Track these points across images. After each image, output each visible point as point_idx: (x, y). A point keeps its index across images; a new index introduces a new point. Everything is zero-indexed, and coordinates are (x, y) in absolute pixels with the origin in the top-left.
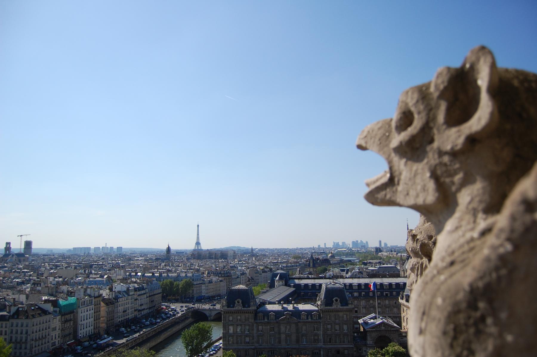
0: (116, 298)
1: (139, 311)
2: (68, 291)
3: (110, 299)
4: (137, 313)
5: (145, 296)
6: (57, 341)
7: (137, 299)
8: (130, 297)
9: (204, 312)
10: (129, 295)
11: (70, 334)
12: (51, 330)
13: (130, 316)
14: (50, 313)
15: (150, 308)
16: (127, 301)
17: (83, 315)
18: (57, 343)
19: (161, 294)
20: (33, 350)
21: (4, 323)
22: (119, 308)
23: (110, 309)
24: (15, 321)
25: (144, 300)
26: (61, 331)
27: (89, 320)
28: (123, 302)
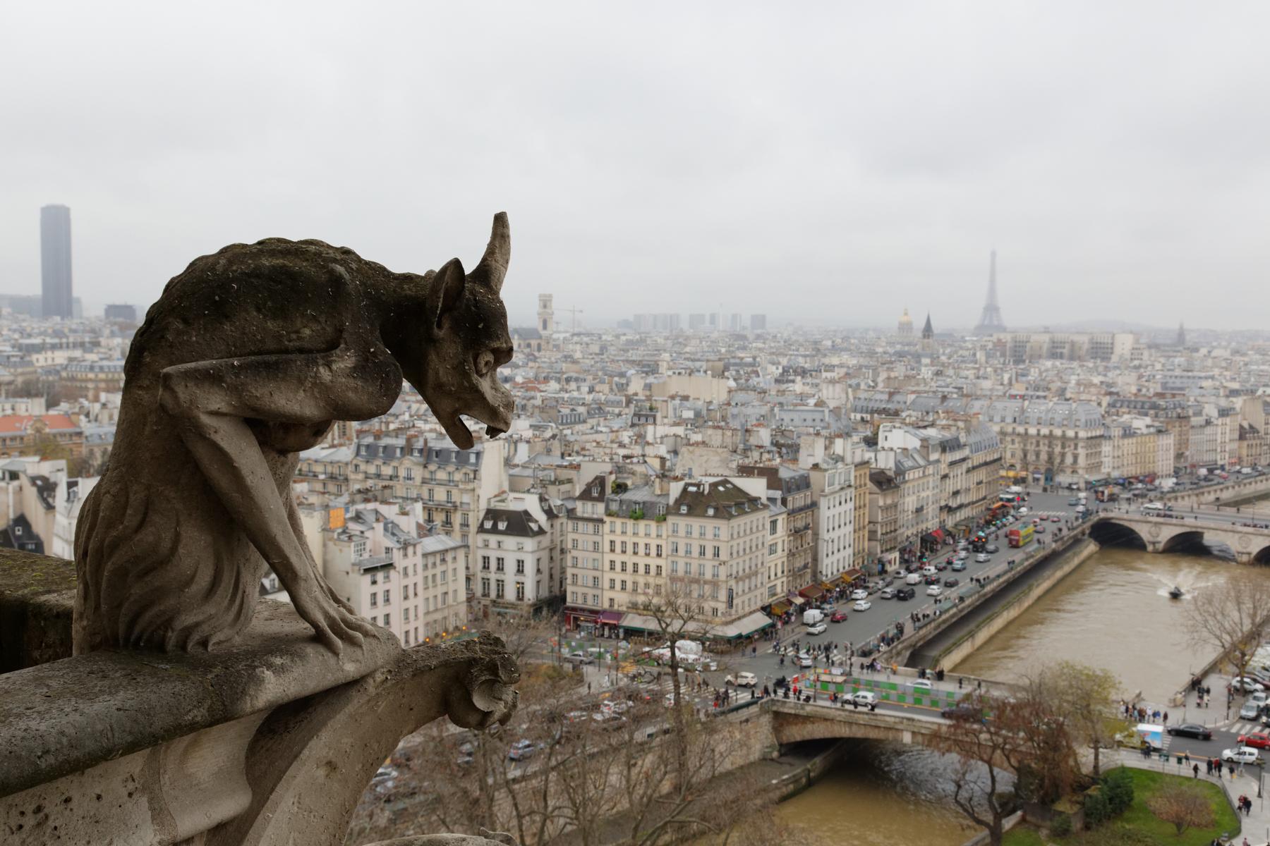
0: (900, 471)
1: (950, 510)
3: (882, 472)
4: (944, 515)
5: (965, 466)
6: (779, 583)
7: (945, 477)
8: (930, 470)
11: (805, 566)
12: (766, 551)
13: (931, 524)
14: (765, 507)
18: (779, 589)
20: (735, 602)
21: (653, 524)
23: (889, 501)
24: (681, 523)
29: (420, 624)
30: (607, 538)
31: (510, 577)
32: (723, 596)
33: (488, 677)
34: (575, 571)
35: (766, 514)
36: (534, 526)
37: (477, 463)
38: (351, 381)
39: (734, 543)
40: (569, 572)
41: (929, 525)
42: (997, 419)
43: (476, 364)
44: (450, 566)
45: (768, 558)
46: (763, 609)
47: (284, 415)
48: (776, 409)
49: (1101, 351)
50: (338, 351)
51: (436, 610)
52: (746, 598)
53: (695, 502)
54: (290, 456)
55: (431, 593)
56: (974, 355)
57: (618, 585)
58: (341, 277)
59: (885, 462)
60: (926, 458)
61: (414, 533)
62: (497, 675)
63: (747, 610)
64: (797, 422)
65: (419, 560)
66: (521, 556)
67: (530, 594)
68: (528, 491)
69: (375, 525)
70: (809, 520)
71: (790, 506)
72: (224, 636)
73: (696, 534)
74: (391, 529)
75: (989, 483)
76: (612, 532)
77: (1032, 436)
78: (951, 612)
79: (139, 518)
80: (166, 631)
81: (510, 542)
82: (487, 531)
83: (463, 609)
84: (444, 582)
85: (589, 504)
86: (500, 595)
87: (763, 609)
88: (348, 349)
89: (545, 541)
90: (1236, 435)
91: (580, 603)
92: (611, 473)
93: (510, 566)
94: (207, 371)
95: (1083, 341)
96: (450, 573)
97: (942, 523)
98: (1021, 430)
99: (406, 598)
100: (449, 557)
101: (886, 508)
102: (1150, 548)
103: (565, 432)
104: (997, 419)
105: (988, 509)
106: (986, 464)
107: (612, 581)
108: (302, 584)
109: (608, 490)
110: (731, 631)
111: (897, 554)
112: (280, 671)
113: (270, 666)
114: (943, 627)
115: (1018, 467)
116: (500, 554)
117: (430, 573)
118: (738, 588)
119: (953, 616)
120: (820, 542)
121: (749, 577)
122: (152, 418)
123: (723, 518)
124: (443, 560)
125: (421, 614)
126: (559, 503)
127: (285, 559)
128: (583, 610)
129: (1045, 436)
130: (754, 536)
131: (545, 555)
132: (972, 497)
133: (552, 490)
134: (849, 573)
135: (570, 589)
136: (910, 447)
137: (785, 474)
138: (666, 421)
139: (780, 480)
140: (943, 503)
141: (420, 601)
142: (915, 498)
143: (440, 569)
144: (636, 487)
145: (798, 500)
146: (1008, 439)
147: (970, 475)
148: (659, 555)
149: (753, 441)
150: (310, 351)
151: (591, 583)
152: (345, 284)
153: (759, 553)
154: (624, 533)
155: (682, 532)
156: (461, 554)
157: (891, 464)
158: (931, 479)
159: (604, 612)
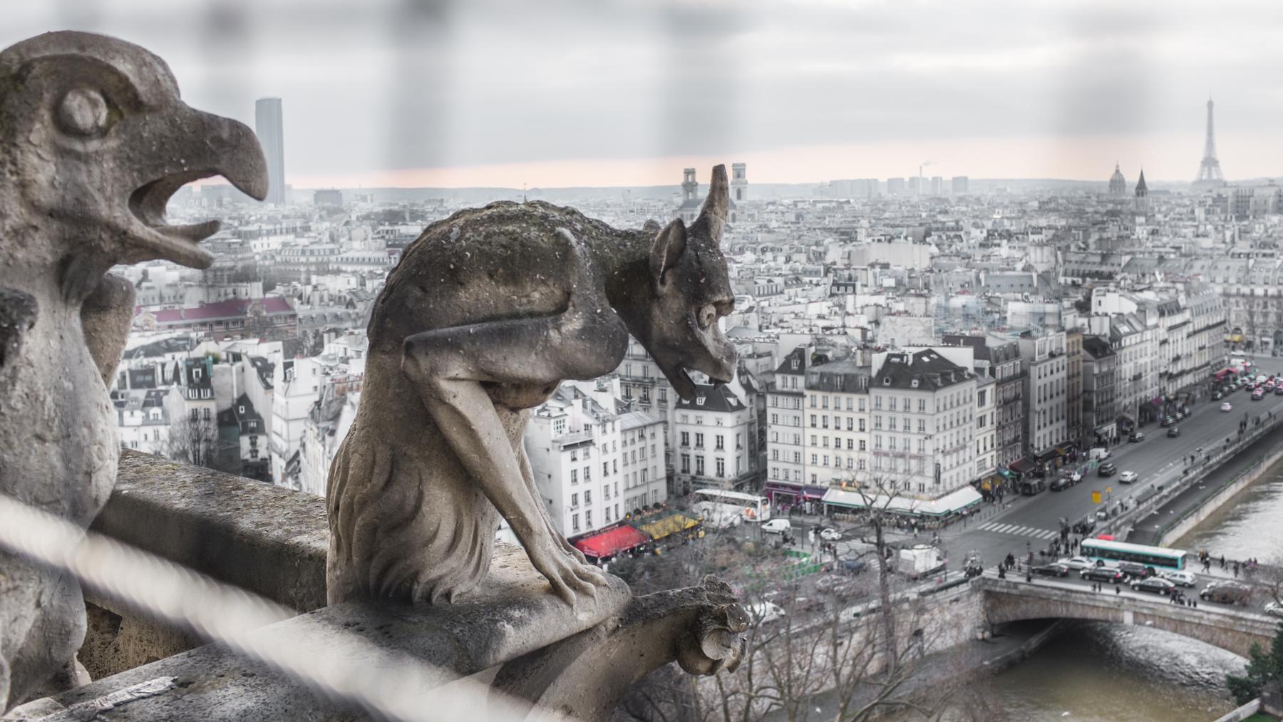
0: (1116, 337)
1: (1171, 377)
4: (1164, 383)
6: (988, 456)
7: (1164, 342)
8: (1148, 335)
10: (1146, 328)
11: (1016, 440)
12: (974, 424)
13: (1151, 392)
14: (972, 377)
16: (1142, 346)
18: (988, 464)
20: (943, 476)
21: (856, 398)
23: (1105, 369)
26: (997, 429)
27: (1056, 400)
28: (1133, 349)
29: (621, 500)
30: (808, 412)
31: (710, 455)
32: (930, 471)
33: (717, 626)
34: (776, 446)
35: (973, 384)
38: (579, 342)
39: (941, 416)
40: (770, 447)
41: (1149, 393)
42: (1219, 279)
43: (698, 318)
44: (649, 442)
45: (976, 432)
46: (973, 483)
47: (518, 379)
48: (982, 276)
50: (566, 314)
51: (636, 486)
52: (953, 473)
53: (898, 374)
54: (522, 412)
55: (630, 469)
56: (1193, 212)
57: (820, 461)
58: (567, 241)
59: (1099, 327)
61: (612, 410)
62: (726, 624)
63: (955, 485)
65: (618, 437)
66: (720, 432)
69: (574, 402)
71: (999, 376)
72: (466, 588)
73: (900, 407)
74: (592, 407)
75: (1212, 348)
76: (813, 406)
77: (1258, 297)
78: (1174, 486)
79: (386, 476)
80: (412, 584)
81: (710, 417)
82: (685, 407)
83: (662, 487)
84: (644, 459)
85: (789, 378)
87: (973, 483)
88: (575, 312)
89: (745, 415)
91: (781, 479)
92: (811, 345)
93: (710, 442)
94: (445, 339)
97: (1162, 391)
98: (1246, 290)
99: (606, 474)
100: (648, 433)
103: (763, 304)
104: (1219, 279)
105: (1211, 375)
106: (1209, 328)
107: (814, 456)
108: (537, 538)
109: (808, 362)
110: (939, 507)
111: (1114, 425)
112: (518, 624)
113: (510, 620)
114: (1165, 501)
115: (1244, 330)
116: (699, 429)
117: (629, 449)
118: (945, 462)
119: (1175, 490)
120: (1031, 414)
121: (956, 451)
122: (394, 381)
123: (929, 389)
124: (642, 437)
125: (621, 491)
127: (520, 514)
128: (785, 486)
129: (1273, 297)
132: (1197, 361)
134: (1061, 446)
135: (770, 465)
136: (1126, 312)
137: (992, 342)
138: (866, 290)
139: (988, 349)
140: (1163, 370)
141: (619, 478)
142: (1132, 365)
143: (639, 445)
146: (1233, 300)
147: (1191, 339)
150: (540, 315)
151: (792, 459)
152: (572, 247)
153: (967, 426)
154: (825, 407)
155: (885, 405)
156: (659, 430)
157: (1106, 330)
158: (1148, 345)
159: (807, 488)
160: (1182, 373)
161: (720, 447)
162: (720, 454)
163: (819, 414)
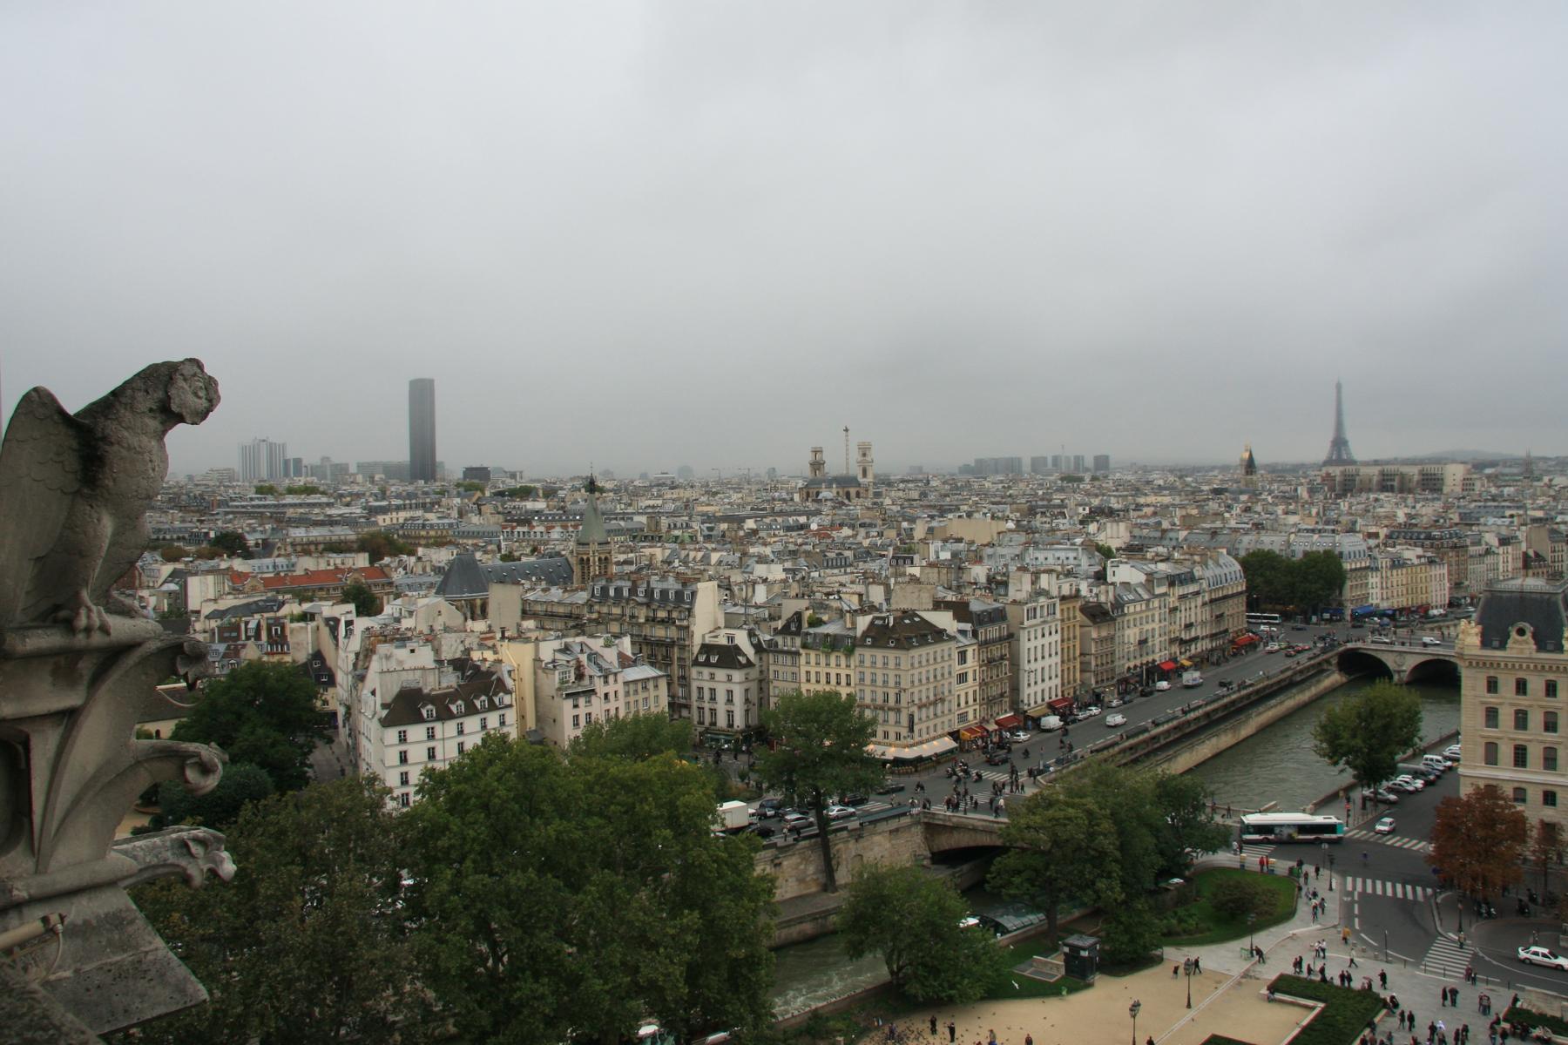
0: (1119, 605)
1: (1182, 642)
2: (990, 579)
3: (1099, 605)
4: (1175, 649)
5: (1199, 600)
7: (1174, 610)
9: (1379, 655)
11: (1002, 695)
12: (954, 680)
13: (1159, 657)
15: (1213, 636)
17: (1032, 644)
18: (971, 717)
19: (1243, 599)
20: (916, 728)
22: (1127, 632)
23: (1104, 633)
24: (868, 654)
25: (1195, 612)
27: (1048, 661)
31: (721, 708)
32: (904, 720)
35: (953, 645)
36: (742, 660)
37: (692, 603)
39: (916, 672)
41: (1157, 657)
44: (652, 693)
49: (1431, 483)
52: (931, 724)
53: (880, 636)
59: (1105, 596)
60: (1150, 591)
63: (933, 734)
64: (1051, 560)
67: (739, 722)
68: (740, 628)
70: (1005, 651)
71: (982, 637)
73: (879, 664)
78: (1141, 737)
81: (721, 674)
86: (714, 724)
89: (754, 673)
90: (1520, 565)
93: (721, 697)
95: (1413, 472)
96: (652, 699)
100: (651, 685)
101: (1101, 641)
102: (1396, 677)
109: (805, 625)
110: (909, 754)
117: (632, 699)
121: (935, 703)
124: (645, 688)
126: (768, 637)
130: (938, 666)
131: (754, 686)
133: (763, 625)
137: (976, 606)
142: (1137, 630)
143: (641, 695)
144: (830, 621)
145: (993, 631)
148: (848, 684)
149: (965, 578)
153: (946, 683)
155: (868, 663)
160: (1196, 639)
161: (730, 701)
162: (730, 708)
163: (813, 671)
